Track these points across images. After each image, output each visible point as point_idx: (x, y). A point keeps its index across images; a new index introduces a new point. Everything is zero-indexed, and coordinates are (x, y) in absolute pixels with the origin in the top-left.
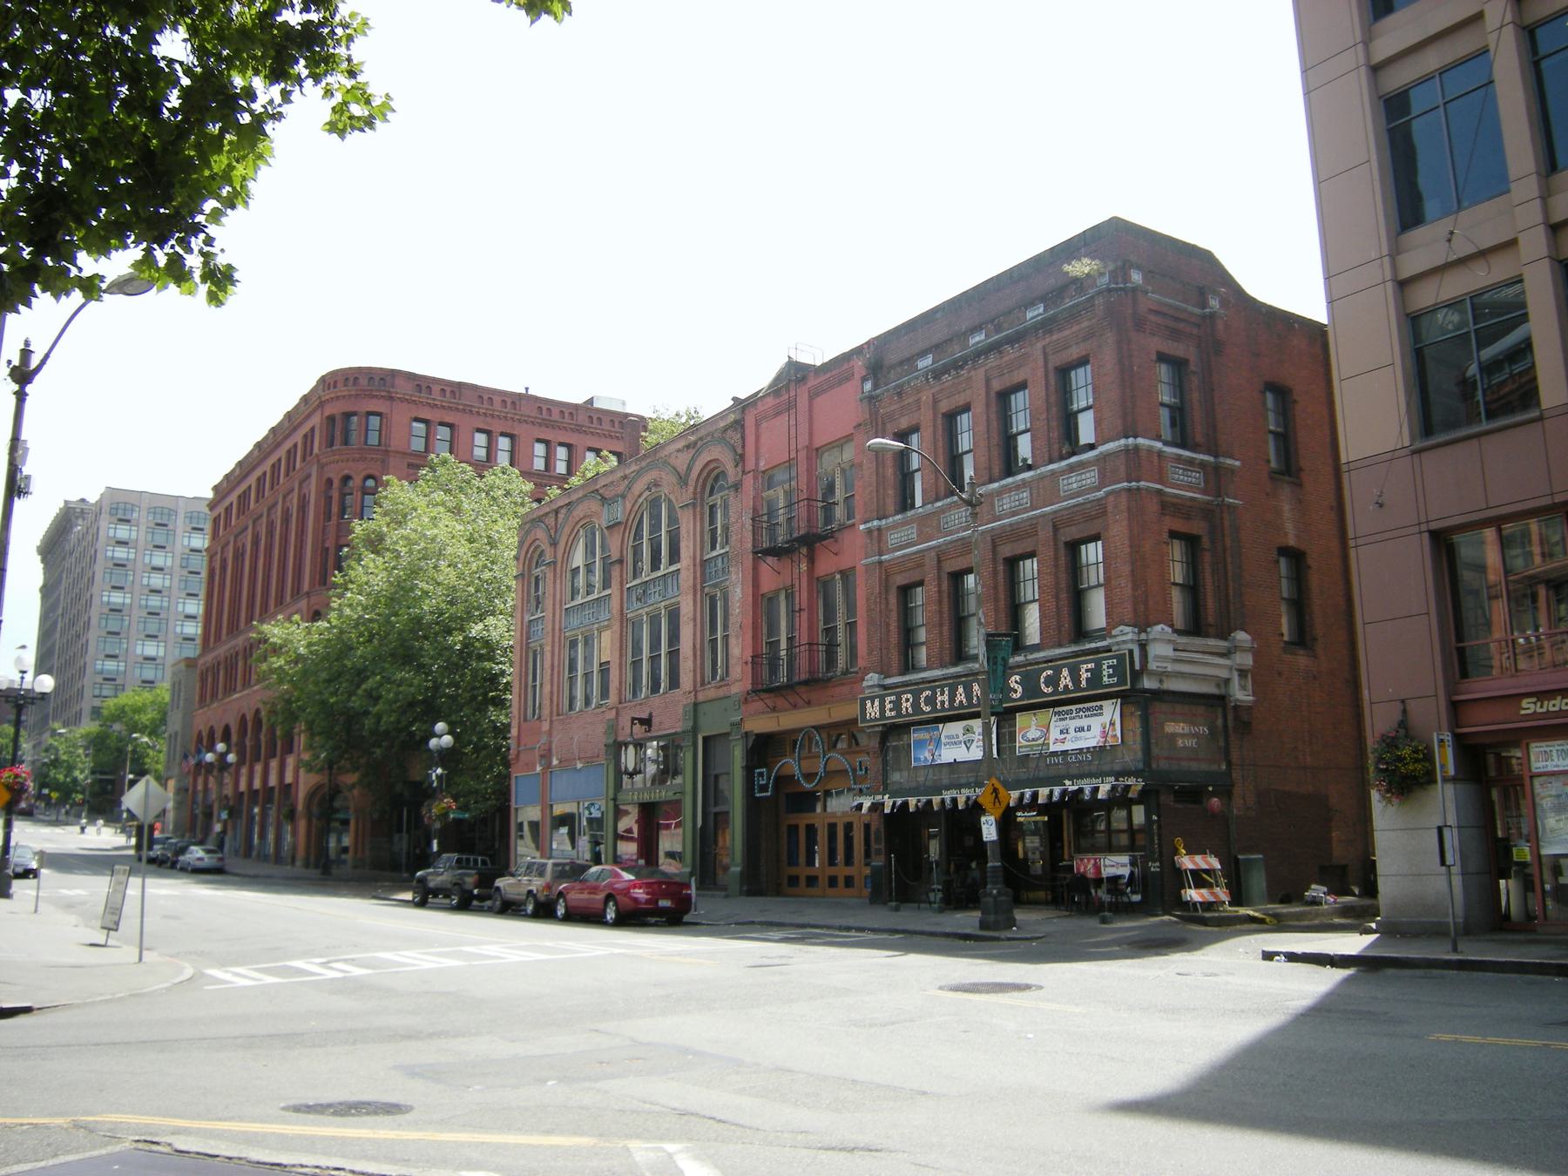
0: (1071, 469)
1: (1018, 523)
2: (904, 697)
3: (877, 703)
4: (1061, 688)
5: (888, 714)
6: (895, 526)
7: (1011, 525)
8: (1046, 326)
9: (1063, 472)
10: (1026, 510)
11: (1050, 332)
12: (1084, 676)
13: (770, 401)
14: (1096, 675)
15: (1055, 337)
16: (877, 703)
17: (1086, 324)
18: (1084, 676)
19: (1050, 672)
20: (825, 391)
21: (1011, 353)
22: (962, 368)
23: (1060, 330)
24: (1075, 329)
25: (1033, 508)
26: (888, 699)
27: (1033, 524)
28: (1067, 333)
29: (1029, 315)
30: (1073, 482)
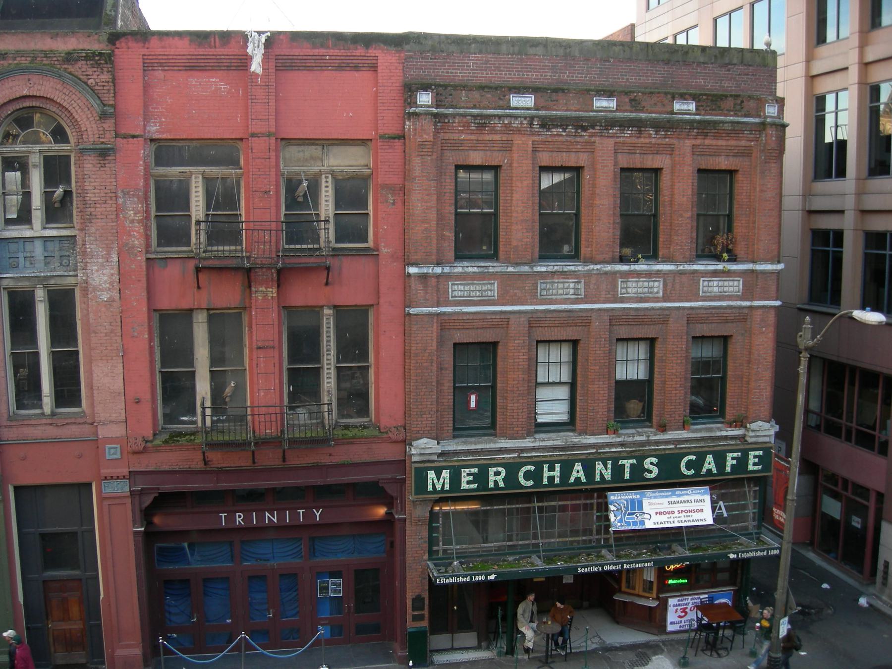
0: (715, 273)
1: (647, 309)
2: (492, 470)
3: (446, 474)
4: (704, 470)
5: (464, 486)
6: (463, 277)
7: (637, 309)
8: (703, 128)
9: (705, 274)
10: (657, 300)
11: (706, 135)
12: (730, 462)
13: (183, 48)
14: (742, 462)
15: (707, 142)
16: (446, 474)
17: (743, 143)
18: (730, 462)
19: (693, 457)
20: (309, 69)
21: (652, 137)
22: (584, 129)
23: (716, 138)
24: (733, 143)
25: (665, 299)
26: (464, 472)
27: (663, 317)
28: (720, 142)
29: (677, 106)
30: (715, 286)
